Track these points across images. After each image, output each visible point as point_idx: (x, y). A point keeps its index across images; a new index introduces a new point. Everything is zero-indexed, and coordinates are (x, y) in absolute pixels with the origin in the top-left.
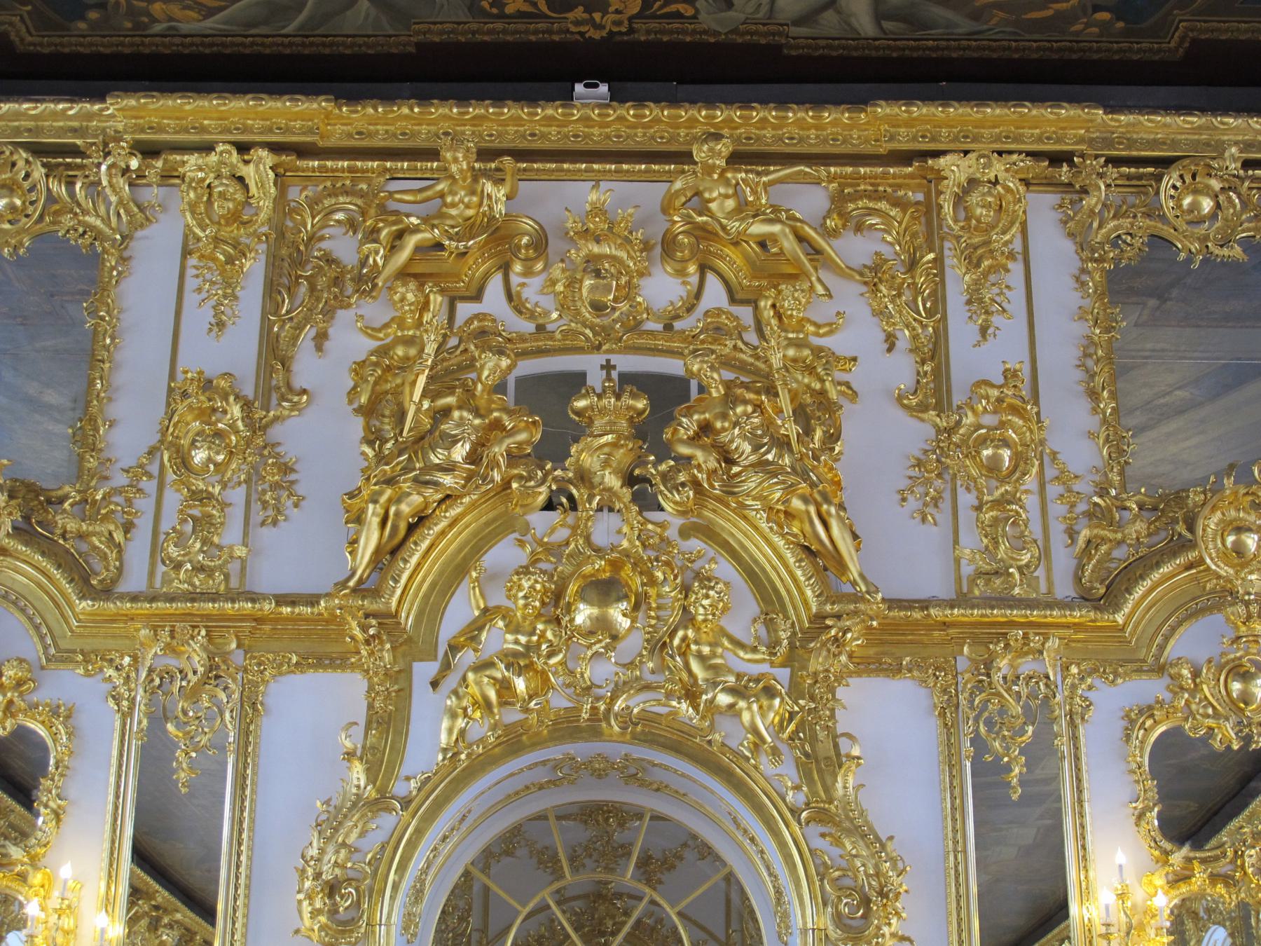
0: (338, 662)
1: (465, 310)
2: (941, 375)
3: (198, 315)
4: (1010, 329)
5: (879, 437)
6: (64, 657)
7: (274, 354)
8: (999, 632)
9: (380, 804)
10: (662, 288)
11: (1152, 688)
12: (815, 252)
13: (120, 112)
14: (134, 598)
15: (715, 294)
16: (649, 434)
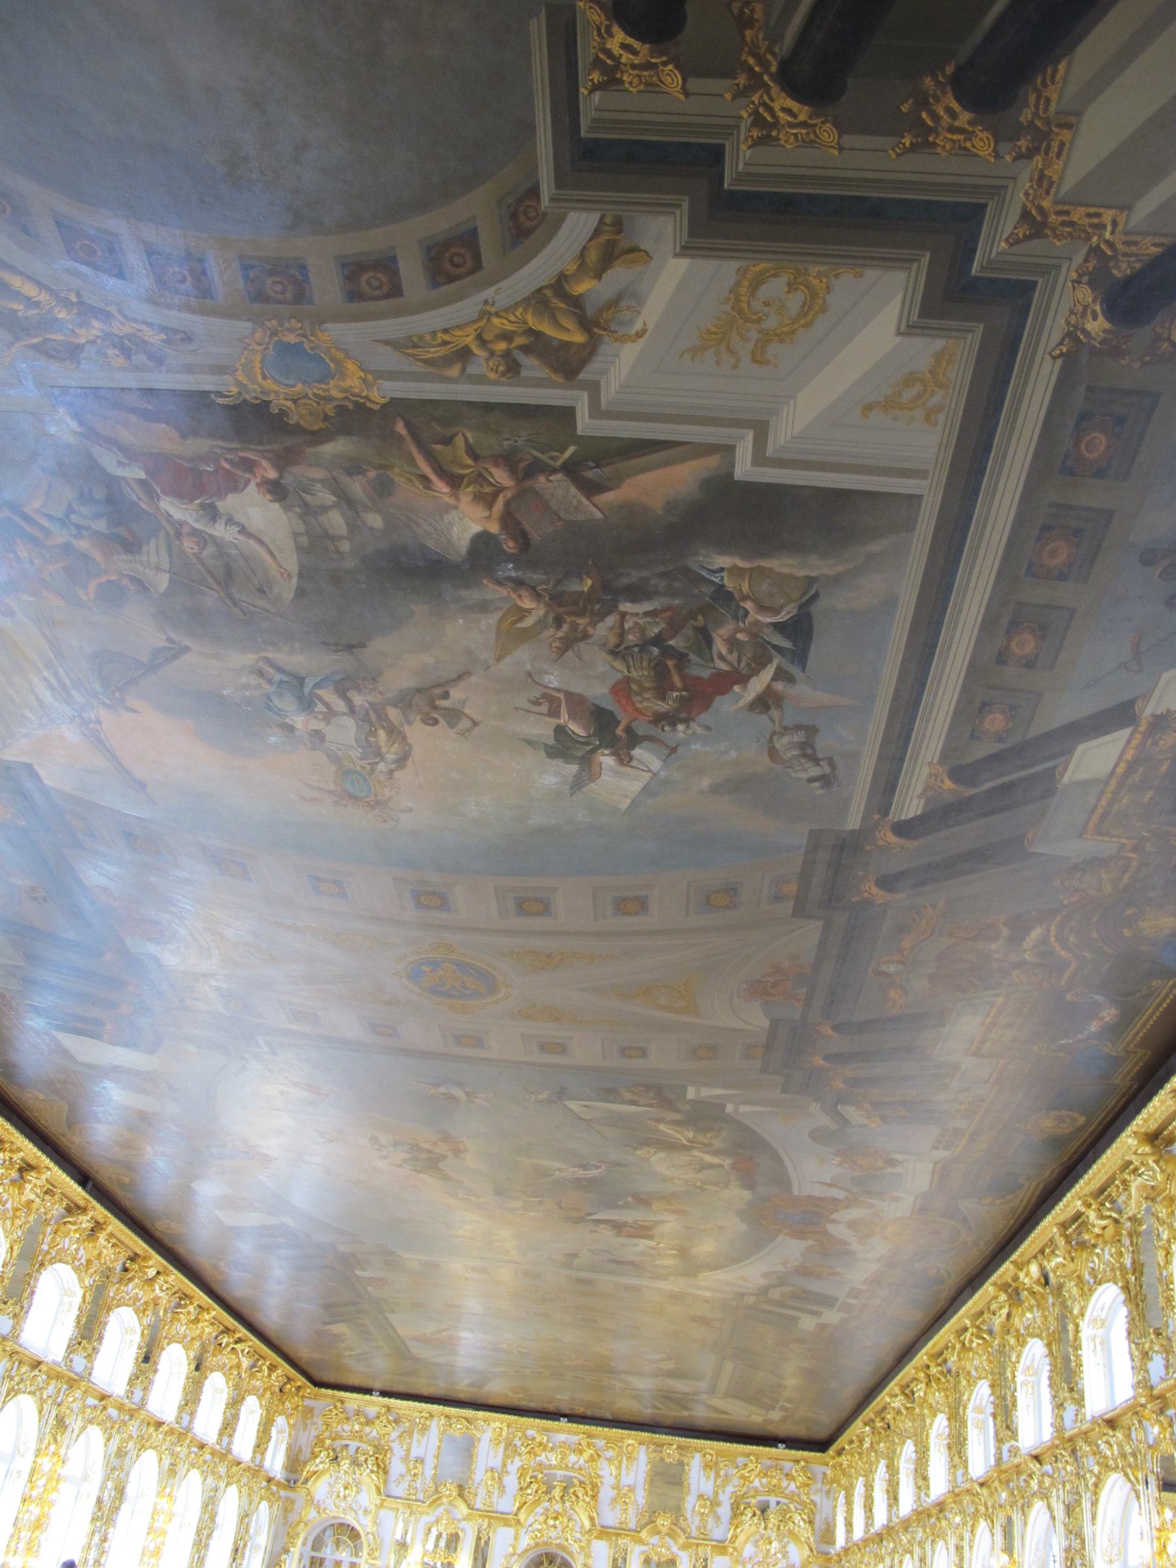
0: (510, 1526)
1: (538, 1459)
2: (619, 1481)
3: (492, 1454)
4: (632, 1474)
5: (606, 1493)
6: (464, 1519)
7: (504, 1465)
8: (620, 1535)
9: (514, 1554)
10: (573, 1458)
11: (645, 1548)
12: (599, 1456)
13: (481, 1414)
14: (478, 1510)
15: (582, 1462)
16: (565, 1489)
